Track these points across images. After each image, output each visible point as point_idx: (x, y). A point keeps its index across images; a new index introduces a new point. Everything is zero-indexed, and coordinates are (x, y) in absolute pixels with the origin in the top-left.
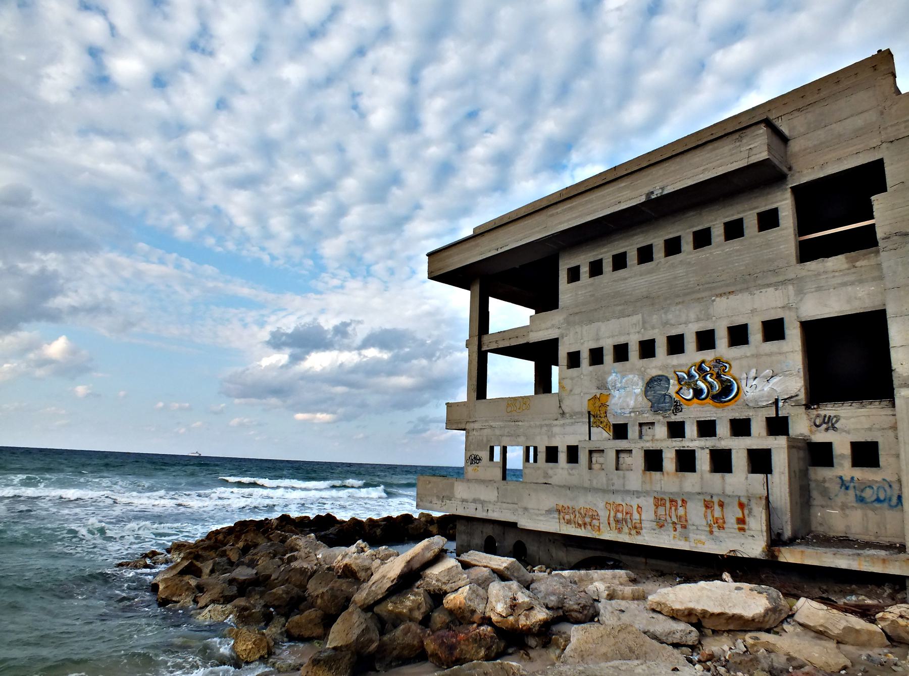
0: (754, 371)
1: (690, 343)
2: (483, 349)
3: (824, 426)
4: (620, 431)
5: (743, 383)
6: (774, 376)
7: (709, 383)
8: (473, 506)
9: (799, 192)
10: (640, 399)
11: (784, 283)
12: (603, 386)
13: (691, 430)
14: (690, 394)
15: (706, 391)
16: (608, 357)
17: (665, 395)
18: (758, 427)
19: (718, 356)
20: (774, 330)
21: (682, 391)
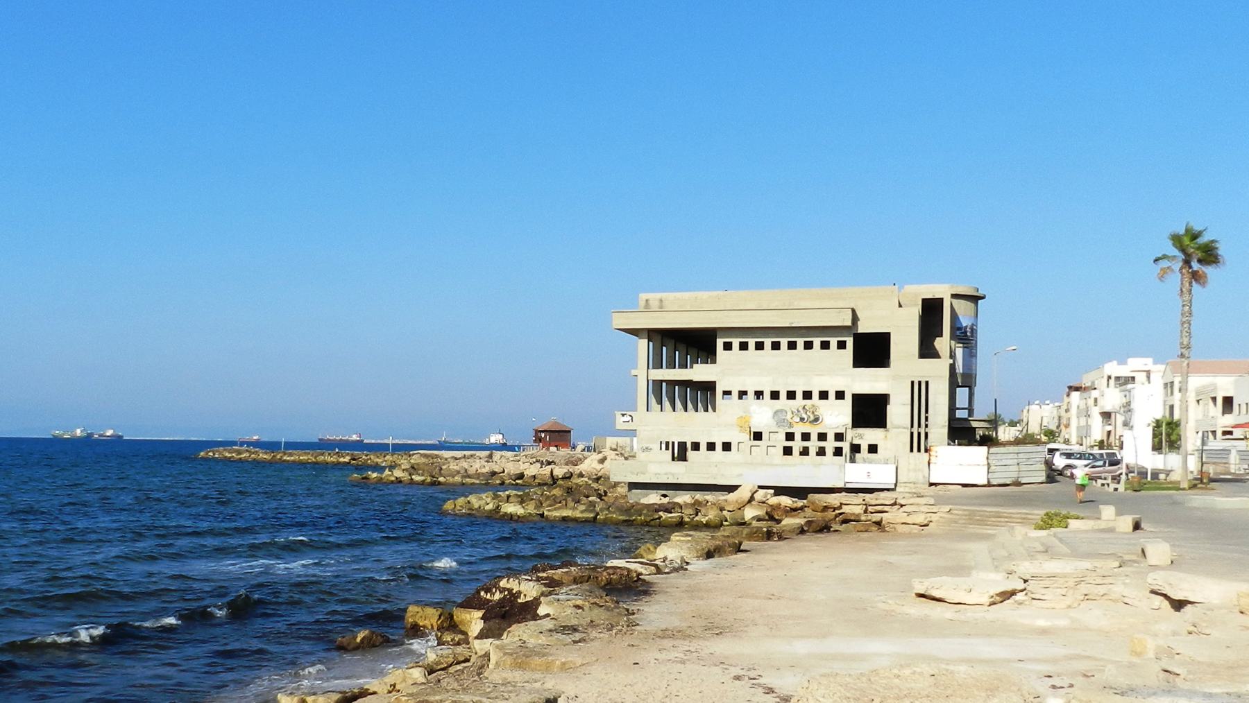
1: (799, 395)
4: (758, 436)
6: (838, 416)
13: (798, 437)
18: (831, 437)
20: (840, 395)
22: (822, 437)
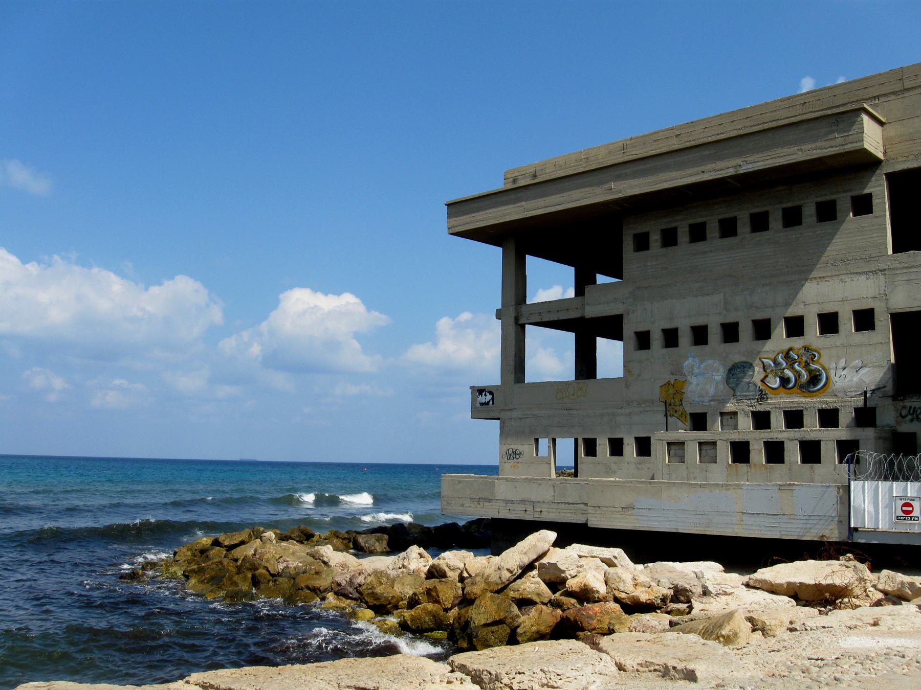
0: (843, 360)
2: (521, 322)
3: (910, 417)
5: (832, 373)
7: (797, 371)
8: (523, 507)
9: (893, 179)
10: (721, 386)
11: (874, 272)
12: (678, 370)
13: (778, 420)
14: (775, 383)
15: (793, 380)
16: (685, 338)
17: (749, 383)
18: (846, 417)
19: (807, 344)
20: (865, 320)
21: (768, 379)
22: (829, 418)
